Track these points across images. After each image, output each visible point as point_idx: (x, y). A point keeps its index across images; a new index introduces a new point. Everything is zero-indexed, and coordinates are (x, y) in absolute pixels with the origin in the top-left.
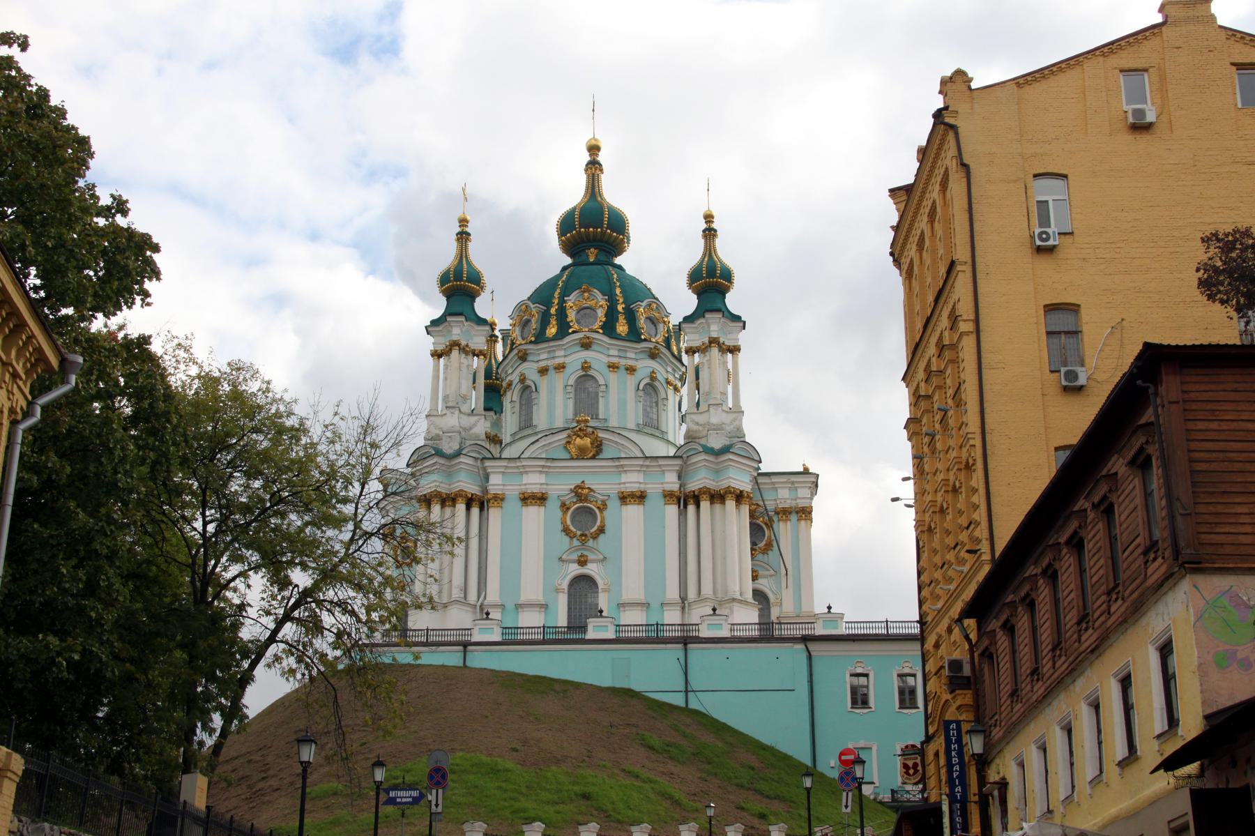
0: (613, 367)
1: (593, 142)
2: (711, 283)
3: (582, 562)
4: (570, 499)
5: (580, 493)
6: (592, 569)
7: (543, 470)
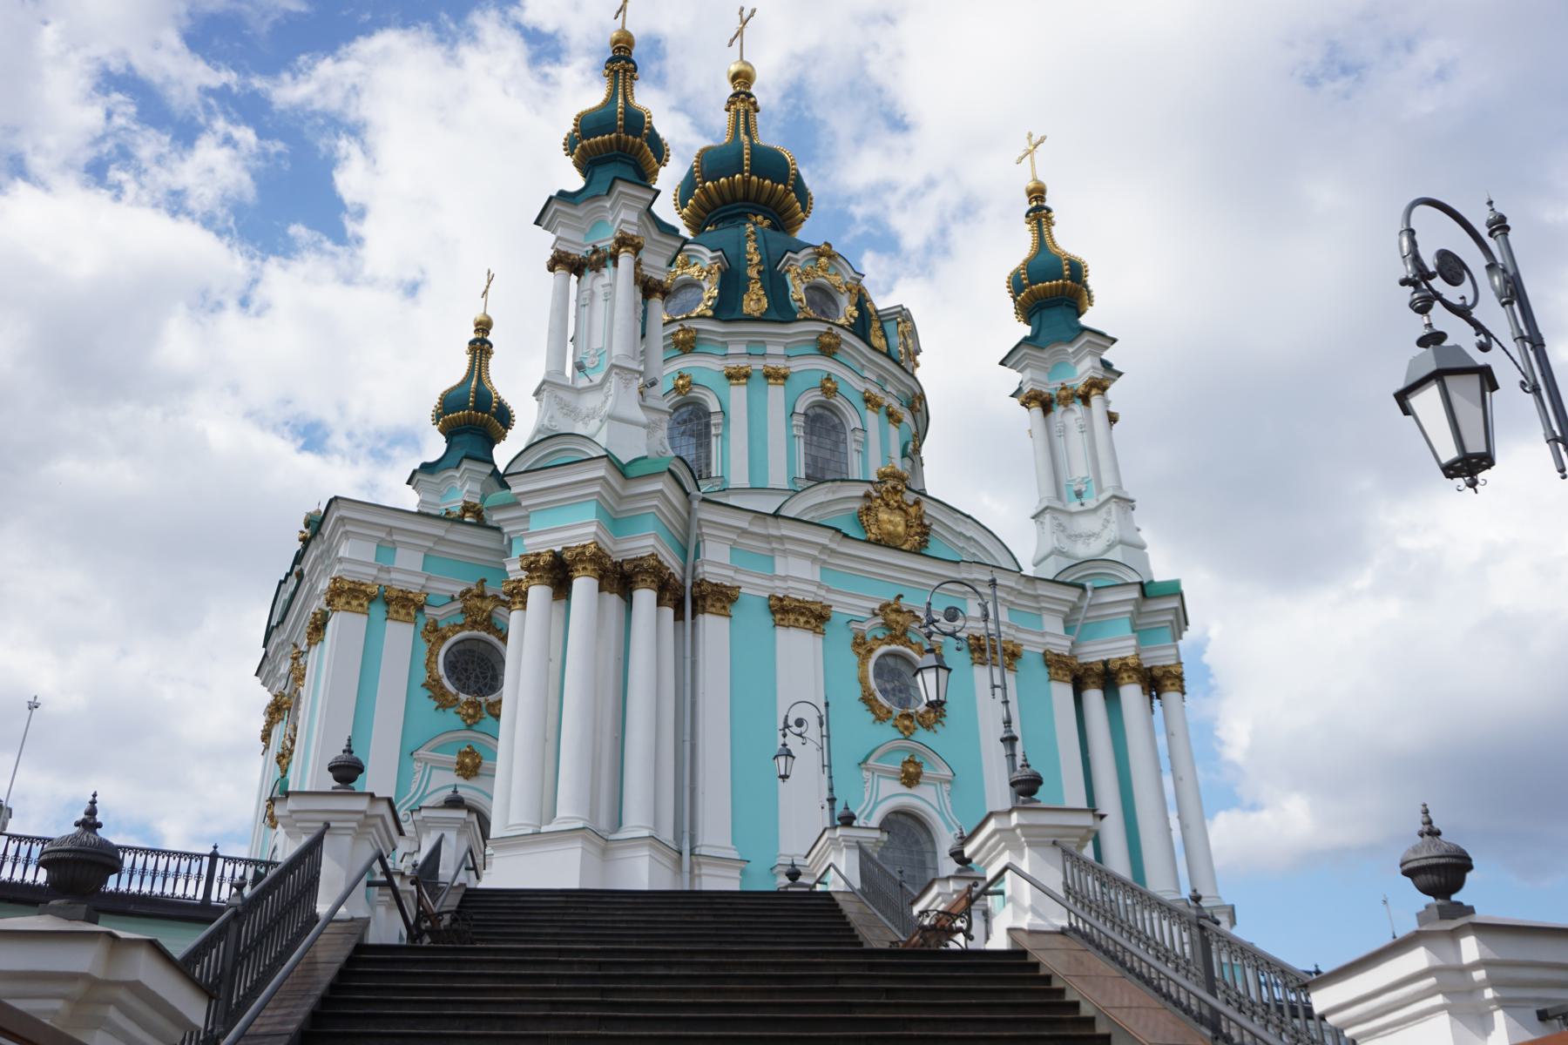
0: (868, 400)
1: (742, 67)
2: (1052, 295)
3: (911, 778)
6: (924, 799)
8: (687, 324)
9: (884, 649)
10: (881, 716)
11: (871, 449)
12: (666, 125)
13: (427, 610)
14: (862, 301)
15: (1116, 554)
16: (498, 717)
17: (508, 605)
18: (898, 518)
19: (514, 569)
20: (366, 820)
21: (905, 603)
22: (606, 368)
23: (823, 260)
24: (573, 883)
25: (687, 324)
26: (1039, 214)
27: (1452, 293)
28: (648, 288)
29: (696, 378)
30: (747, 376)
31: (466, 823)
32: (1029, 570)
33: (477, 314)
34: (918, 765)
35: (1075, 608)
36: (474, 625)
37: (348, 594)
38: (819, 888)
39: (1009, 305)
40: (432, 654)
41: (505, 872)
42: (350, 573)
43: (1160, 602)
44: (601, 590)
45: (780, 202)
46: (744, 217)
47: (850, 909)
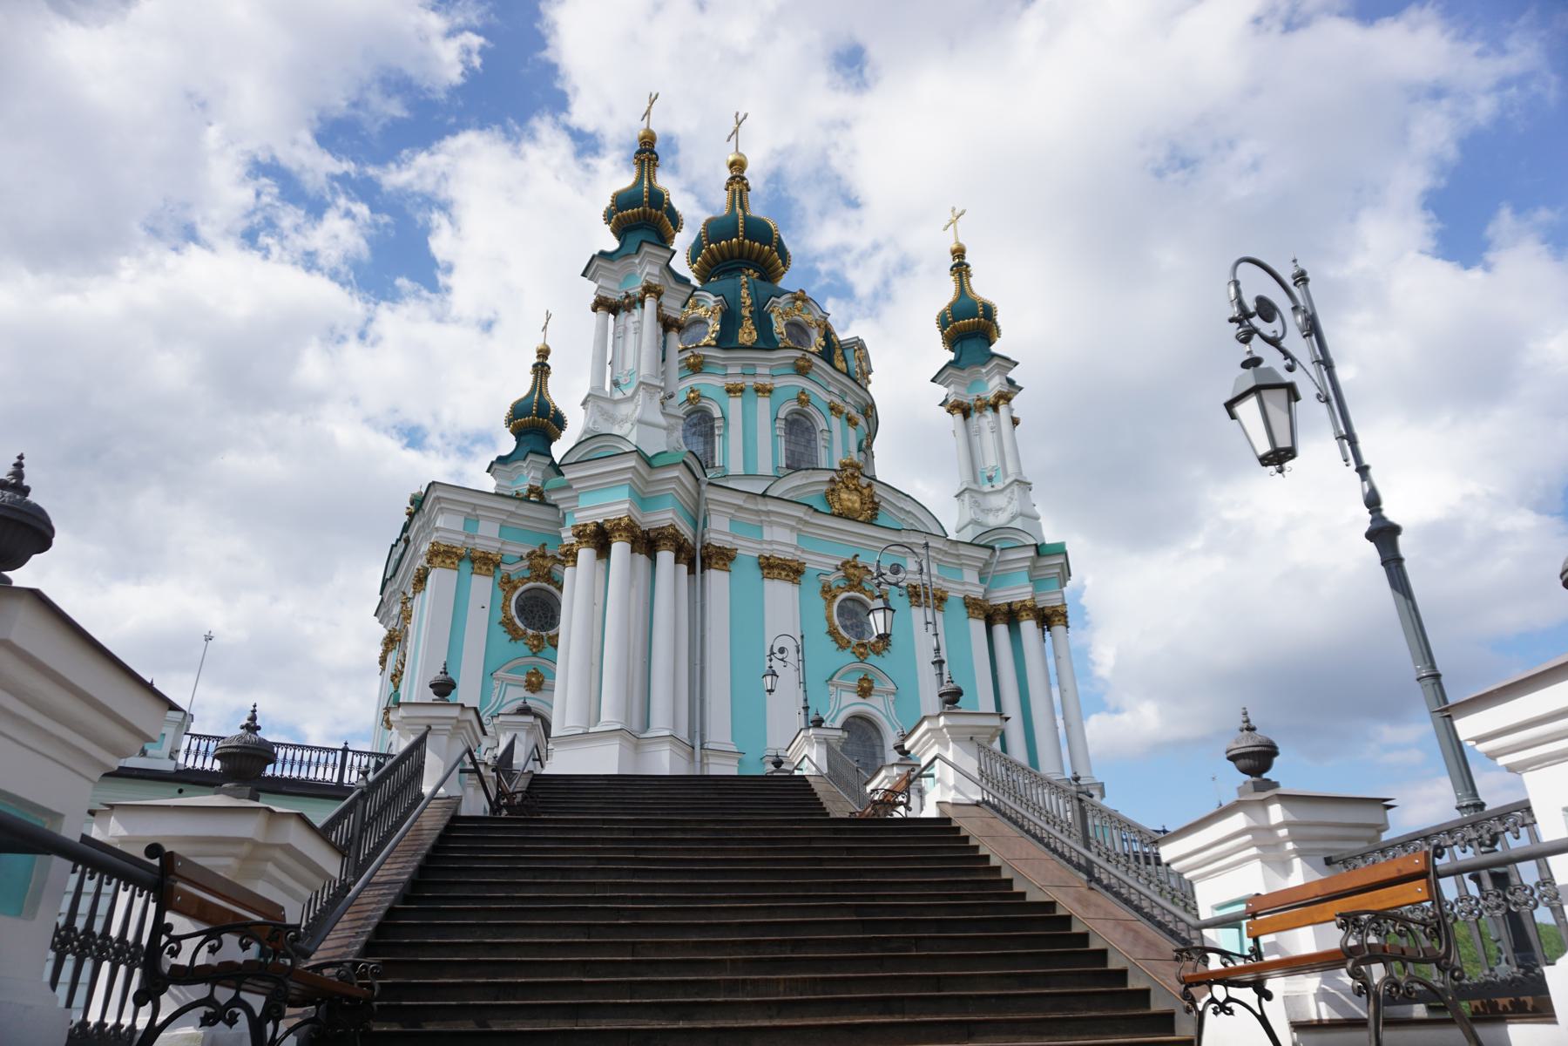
0: (833, 409)
2: (970, 329)
3: (865, 691)
4: (835, 579)
5: (853, 573)
6: (875, 707)
7: (799, 527)
8: (696, 351)
9: (845, 595)
10: (842, 645)
11: (835, 446)
12: (680, 202)
13: (503, 567)
14: (828, 334)
15: (1017, 524)
16: (556, 647)
17: (563, 564)
18: (855, 497)
19: (568, 536)
20: (459, 724)
21: (861, 561)
22: (635, 384)
23: (799, 303)
24: (615, 772)
25: (696, 351)
26: (961, 269)
27: (1267, 329)
28: (667, 324)
29: (704, 392)
30: (742, 390)
31: (533, 726)
32: (952, 536)
33: (539, 344)
34: (870, 681)
35: (987, 564)
36: (538, 578)
37: (443, 554)
38: (797, 773)
39: (937, 336)
40: (507, 599)
41: (561, 763)
42: (445, 539)
43: (1050, 560)
44: (633, 551)
45: (766, 259)
46: (740, 270)
47: (820, 788)
